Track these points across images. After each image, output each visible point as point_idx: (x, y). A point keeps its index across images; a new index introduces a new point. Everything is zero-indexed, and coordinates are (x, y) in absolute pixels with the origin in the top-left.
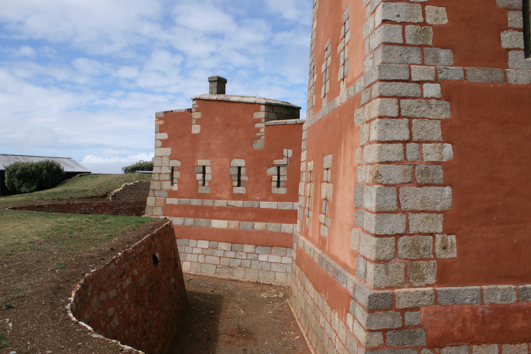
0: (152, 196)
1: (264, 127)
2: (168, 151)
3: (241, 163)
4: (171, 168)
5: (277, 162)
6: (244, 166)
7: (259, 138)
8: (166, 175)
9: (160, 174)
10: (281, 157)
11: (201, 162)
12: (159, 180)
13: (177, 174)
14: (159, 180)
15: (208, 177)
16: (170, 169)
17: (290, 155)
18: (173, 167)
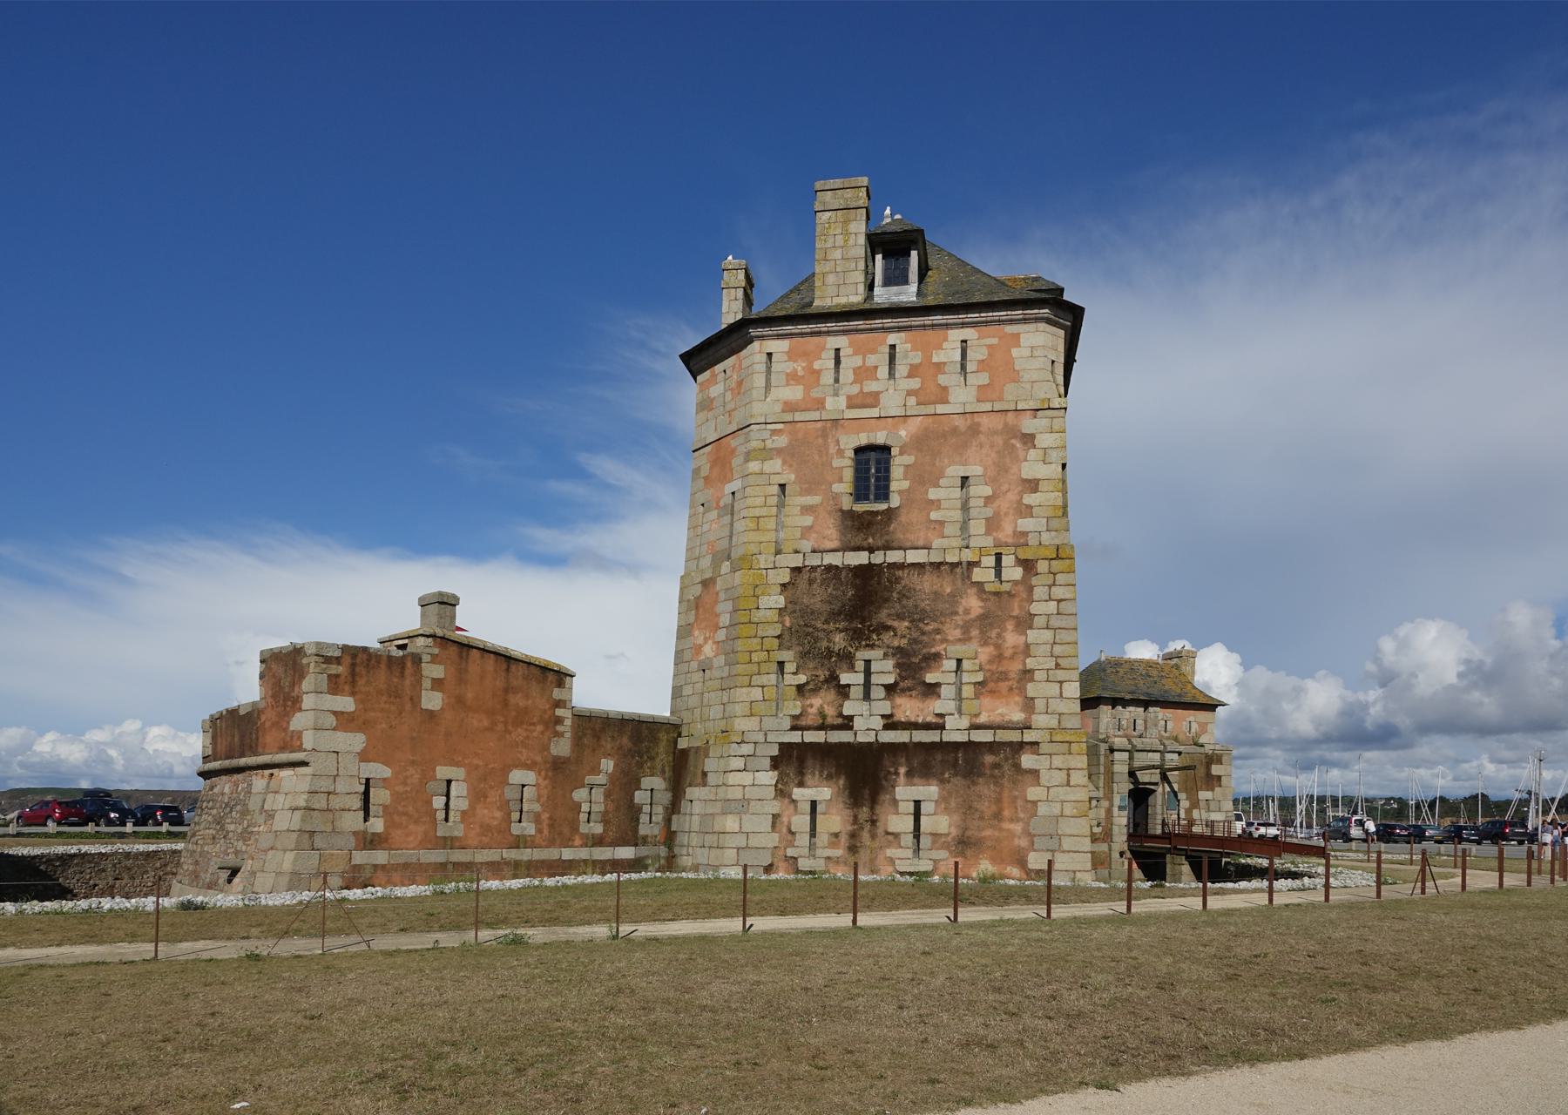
0: (306, 847)
1: (570, 717)
2: (357, 741)
3: (529, 777)
4: (364, 781)
5: (589, 779)
6: (534, 784)
7: (560, 735)
8: (349, 796)
9: (329, 793)
10: (596, 770)
11: (443, 772)
12: (328, 810)
13: (379, 796)
14: (328, 810)
15: (459, 803)
16: (360, 784)
17: (611, 769)
18: (368, 780)
